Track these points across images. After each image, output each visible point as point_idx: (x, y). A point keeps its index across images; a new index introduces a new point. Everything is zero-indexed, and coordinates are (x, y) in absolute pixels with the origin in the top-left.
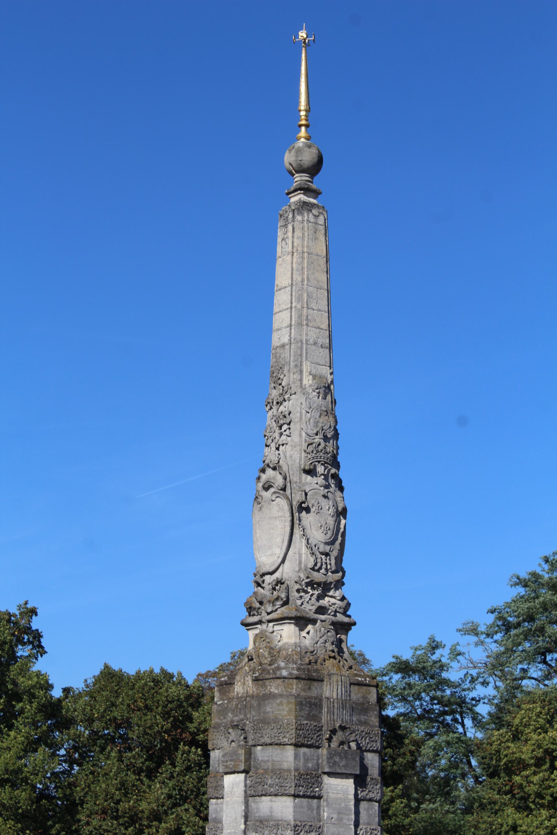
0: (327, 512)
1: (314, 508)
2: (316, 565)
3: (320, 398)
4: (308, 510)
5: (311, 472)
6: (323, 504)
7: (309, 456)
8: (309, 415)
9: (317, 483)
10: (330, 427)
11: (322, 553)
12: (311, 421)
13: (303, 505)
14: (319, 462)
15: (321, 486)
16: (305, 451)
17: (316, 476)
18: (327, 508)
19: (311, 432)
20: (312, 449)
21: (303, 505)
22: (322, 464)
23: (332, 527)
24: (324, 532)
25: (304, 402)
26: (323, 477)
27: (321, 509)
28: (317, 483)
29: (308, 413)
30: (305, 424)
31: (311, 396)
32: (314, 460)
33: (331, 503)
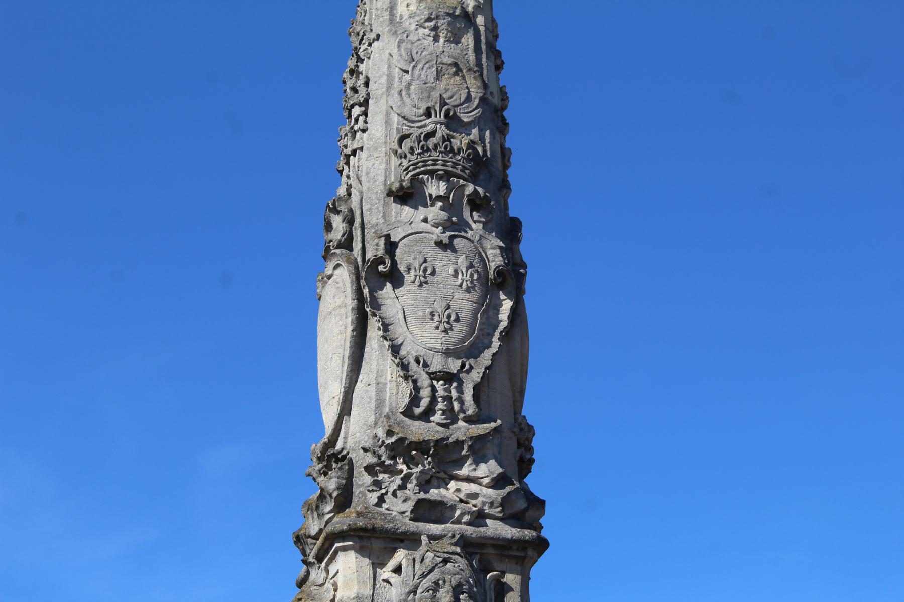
0: (452, 281)
1: (412, 273)
2: (415, 400)
3: (442, 40)
4: (395, 278)
5: (407, 195)
6: (438, 265)
7: (405, 163)
8: (407, 77)
9: (425, 220)
10: (469, 98)
11: (434, 376)
12: (413, 88)
13: (381, 268)
14: (432, 173)
15: (436, 226)
16: (396, 152)
17: (426, 206)
18: (451, 272)
19: (408, 111)
20: (409, 145)
21: (381, 268)
22: (440, 178)
23: (466, 315)
24: (442, 328)
25: (395, 51)
26: (440, 204)
27: (433, 273)
28: (425, 220)
29: (407, 72)
30: (396, 95)
31: (413, 37)
32: (418, 170)
33: (462, 262)
